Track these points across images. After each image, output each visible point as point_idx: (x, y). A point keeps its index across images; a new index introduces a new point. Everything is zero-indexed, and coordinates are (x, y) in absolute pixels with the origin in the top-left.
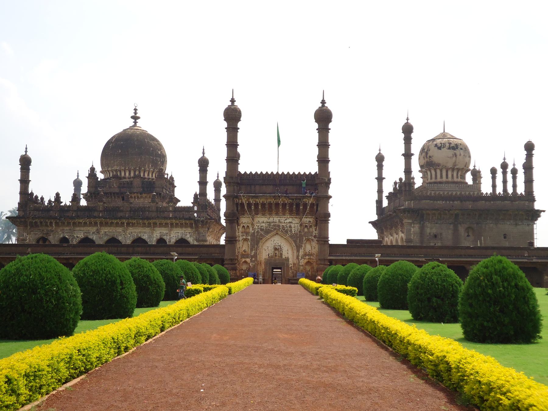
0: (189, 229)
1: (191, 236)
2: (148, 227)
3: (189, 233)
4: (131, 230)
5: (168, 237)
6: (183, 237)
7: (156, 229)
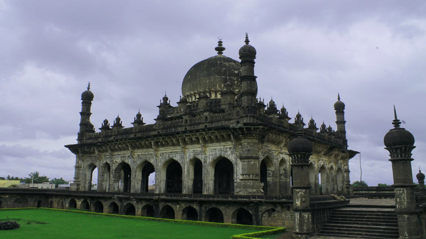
0: (230, 143)
1: (232, 153)
2: (179, 145)
3: (230, 148)
4: (162, 150)
5: (203, 156)
6: (223, 155)
7: (189, 146)
